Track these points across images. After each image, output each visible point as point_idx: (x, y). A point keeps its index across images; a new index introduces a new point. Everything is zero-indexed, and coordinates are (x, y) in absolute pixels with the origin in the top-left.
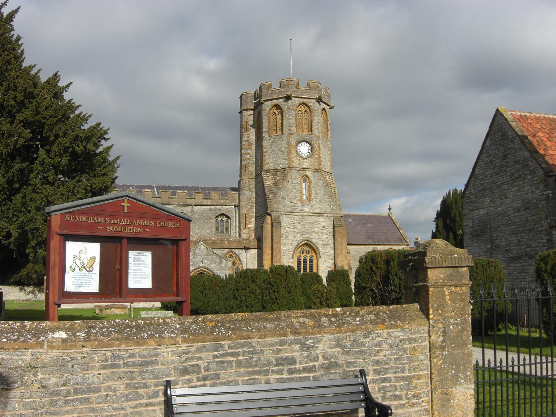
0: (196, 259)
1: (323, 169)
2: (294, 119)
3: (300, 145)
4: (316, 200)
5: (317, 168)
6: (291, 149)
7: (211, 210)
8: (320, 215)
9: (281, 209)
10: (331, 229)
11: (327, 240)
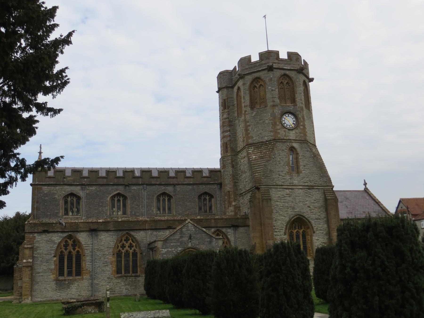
3: (285, 117)
4: (305, 171)
5: (303, 139)
6: (277, 121)
8: (311, 188)
10: (321, 203)
11: (319, 214)
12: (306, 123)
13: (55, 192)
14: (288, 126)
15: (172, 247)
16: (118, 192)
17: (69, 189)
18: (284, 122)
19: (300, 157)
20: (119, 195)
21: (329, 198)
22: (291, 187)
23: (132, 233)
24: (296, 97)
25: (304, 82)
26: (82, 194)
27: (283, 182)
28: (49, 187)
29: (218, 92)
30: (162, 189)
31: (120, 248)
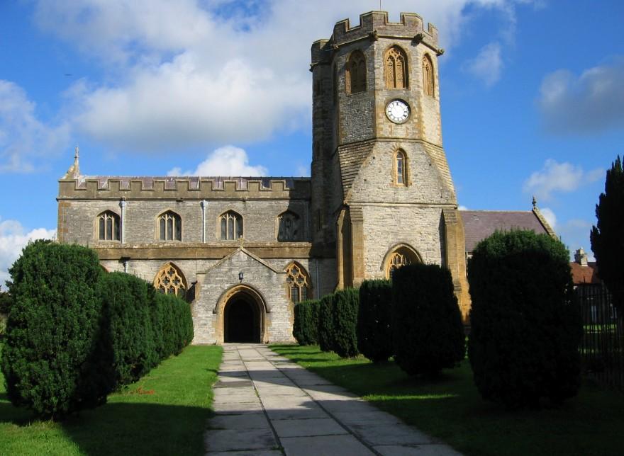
0: (233, 272)
1: (428, 140)
2: (382, 68)
5: (417, 137)
7: (272, 206)
8: (423, 205)
9: (363, 197)
12: (423, 115)
13: (88, 209)
14: (396, 119)
15: (216, 282)
16: (168, 209)
17: (104, 205)
18: (390, 113)
19: (410, 163)
20: (169, 213)
21: (449, 220)
22: (395, 204)
23: (176, 263)
24: (410, 77)
25: (427, 55)
26: (118, 211)
27: (384, 198)
28: (79, 203)
29: (311, 70)
30: (228, 206)
31: (161, 283)
